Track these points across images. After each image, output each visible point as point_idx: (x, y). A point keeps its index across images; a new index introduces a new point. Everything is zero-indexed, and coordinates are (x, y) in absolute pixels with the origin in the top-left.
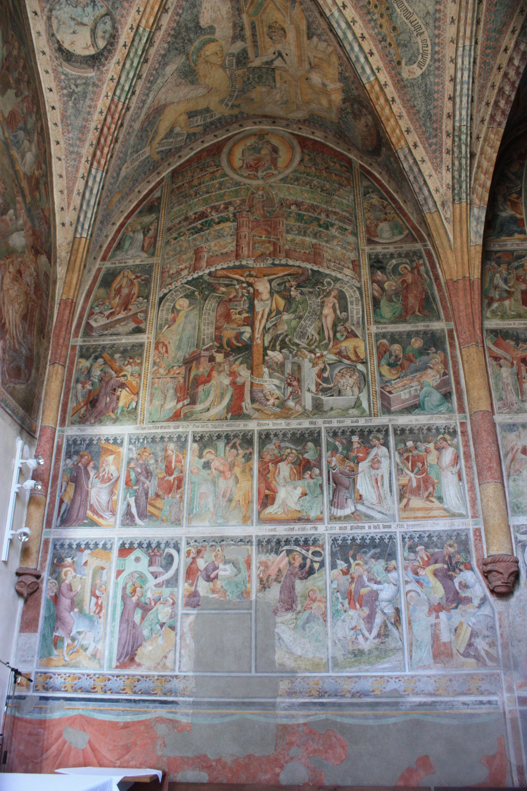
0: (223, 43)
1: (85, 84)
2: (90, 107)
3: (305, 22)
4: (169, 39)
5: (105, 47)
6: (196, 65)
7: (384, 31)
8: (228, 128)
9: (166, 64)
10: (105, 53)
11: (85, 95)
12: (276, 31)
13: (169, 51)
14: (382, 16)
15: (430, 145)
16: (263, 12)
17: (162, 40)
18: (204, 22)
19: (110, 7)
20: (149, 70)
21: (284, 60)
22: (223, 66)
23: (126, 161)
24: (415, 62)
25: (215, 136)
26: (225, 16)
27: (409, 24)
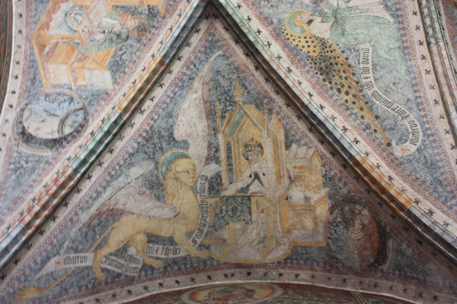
0: (196, 162)
1: (37, 161)
2: (34, 181)
3: (282, 131)
4: (140, 140)
5: (71, 134)
6: (164, 179)
7: (366, 120)
8: (194, 276)
9: (131, 165)
10: (69, 138)
11: (33, 170)
12: (253, 148)
13: (137, 152)
14: (361, 109)
15: (451, 208)
16: (240, 131)
17: (132, 138)
18: (179, 134)
19: (86, 104)
20: (112, 161)
21: (260, 182)
22: (193, 189)
23: (58, 253)
24: (406, 141)
25: (177, 282)
26: (200, 134)
27: (392, 112)
